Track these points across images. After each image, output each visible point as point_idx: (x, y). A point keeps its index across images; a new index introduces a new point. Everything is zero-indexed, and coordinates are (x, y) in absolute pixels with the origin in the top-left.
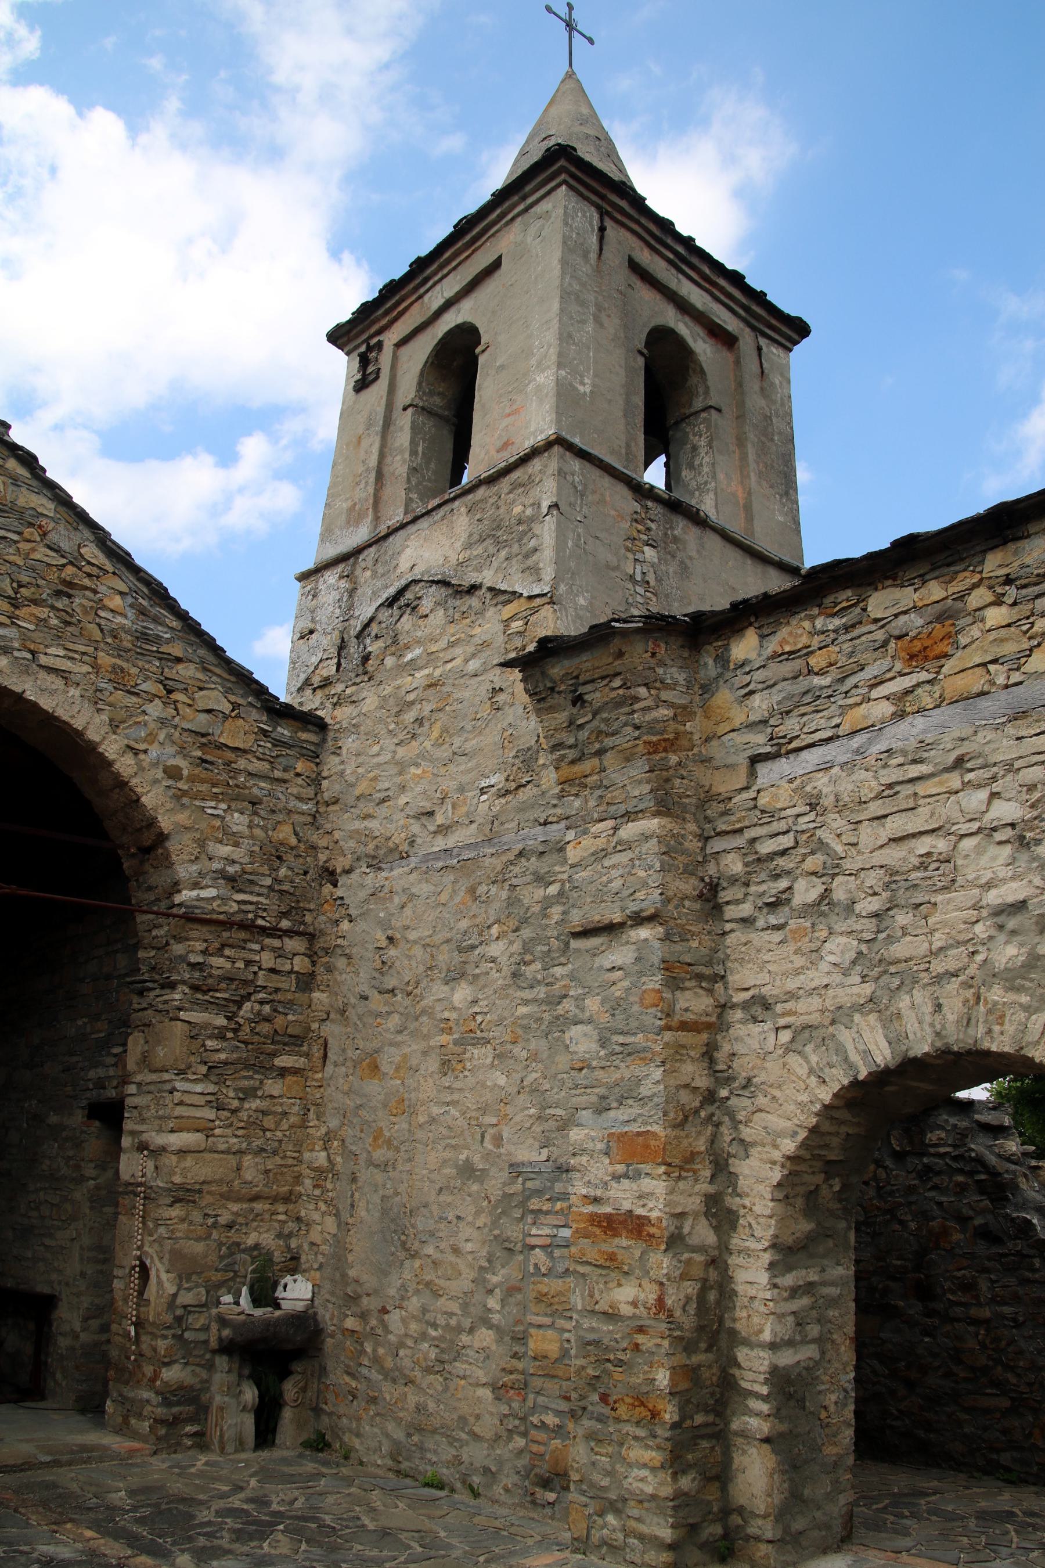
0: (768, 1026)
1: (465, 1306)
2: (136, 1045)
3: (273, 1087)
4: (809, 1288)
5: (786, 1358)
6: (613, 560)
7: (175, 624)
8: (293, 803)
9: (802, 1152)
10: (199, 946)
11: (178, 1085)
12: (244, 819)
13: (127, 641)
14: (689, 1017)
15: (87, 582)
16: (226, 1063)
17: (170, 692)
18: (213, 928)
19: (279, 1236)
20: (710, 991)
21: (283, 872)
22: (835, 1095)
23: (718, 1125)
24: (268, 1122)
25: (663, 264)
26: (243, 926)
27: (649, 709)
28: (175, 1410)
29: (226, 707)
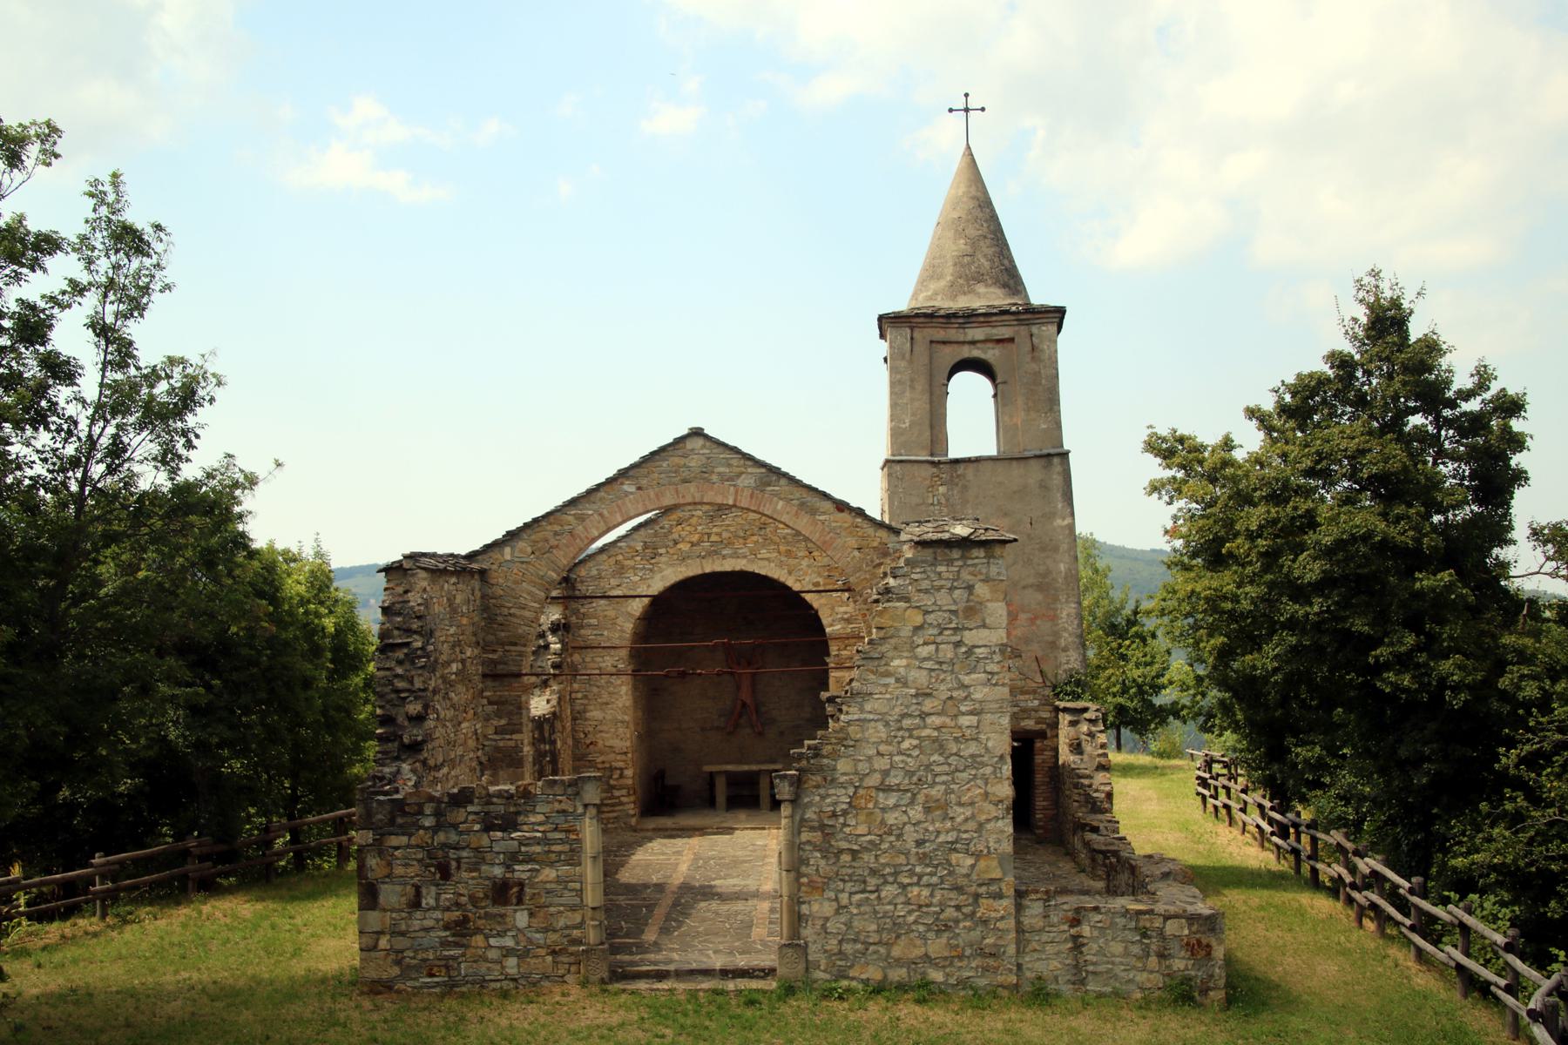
6: (919, 501)
13: (790, 538)
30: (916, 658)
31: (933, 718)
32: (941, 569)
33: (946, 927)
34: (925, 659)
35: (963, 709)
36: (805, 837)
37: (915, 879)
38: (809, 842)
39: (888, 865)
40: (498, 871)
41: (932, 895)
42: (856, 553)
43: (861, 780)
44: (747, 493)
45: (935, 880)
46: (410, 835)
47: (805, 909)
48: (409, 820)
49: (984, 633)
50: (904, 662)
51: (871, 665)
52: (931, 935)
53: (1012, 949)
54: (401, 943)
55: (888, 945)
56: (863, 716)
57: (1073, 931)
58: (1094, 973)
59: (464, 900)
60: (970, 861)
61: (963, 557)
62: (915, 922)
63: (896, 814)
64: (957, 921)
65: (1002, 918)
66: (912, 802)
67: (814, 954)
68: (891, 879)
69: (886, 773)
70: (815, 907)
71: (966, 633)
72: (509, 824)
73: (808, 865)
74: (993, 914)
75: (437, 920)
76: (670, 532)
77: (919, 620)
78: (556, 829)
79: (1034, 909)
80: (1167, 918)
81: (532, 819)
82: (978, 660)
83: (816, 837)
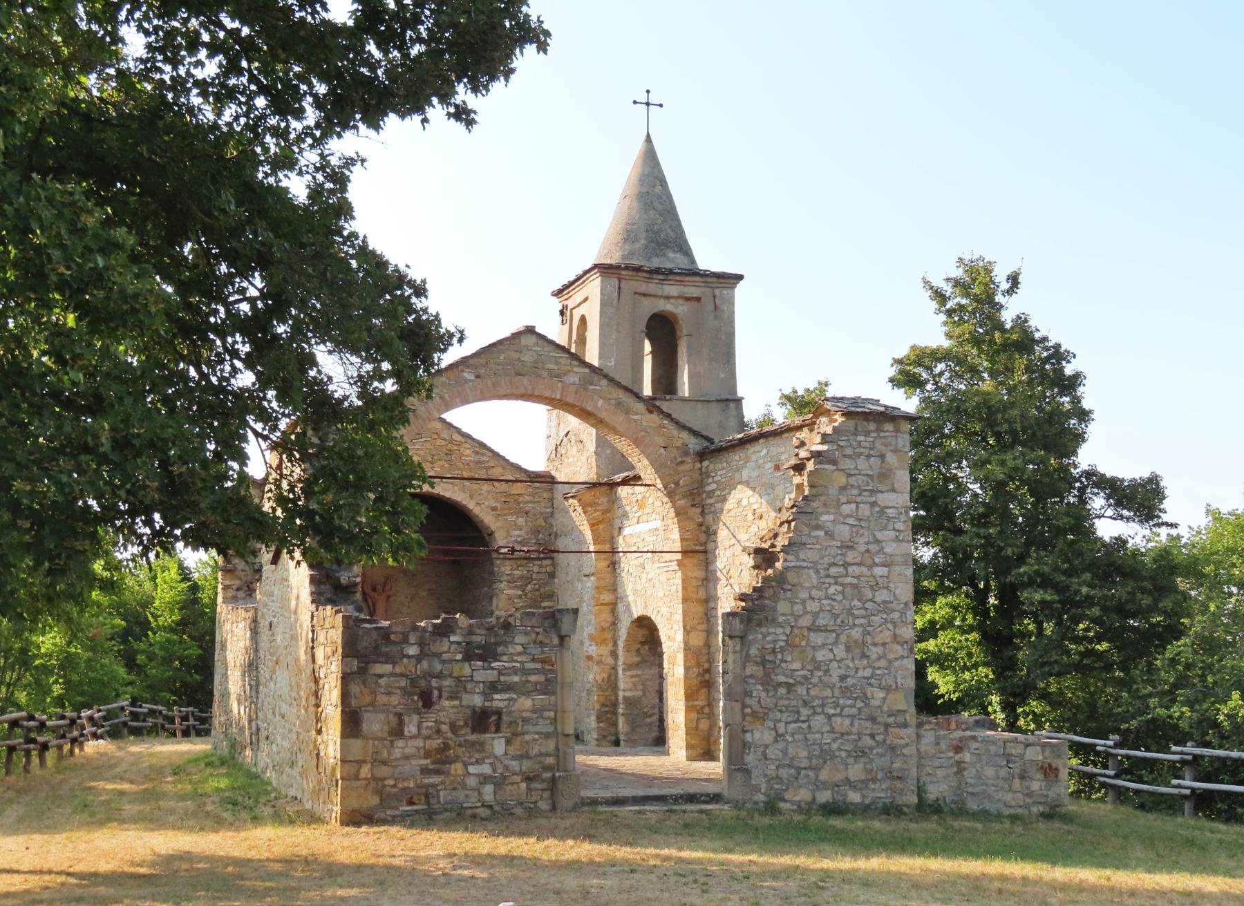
4: (638, 676)
5: (628, 694)
13: (472, 465)
30: (841, 515)
31: (854, 567)
32: (861, 438)
33: (861, 753)
34: (849, 516)
35: (877, 560)
36: (748, 671)
37: (838, 710)
38: (752, 676)
39: (818, 698)
40: (477, 701)
41: (852, 724)
43: (796, 620)
44: (572, 389)
45: (854, 711)
46: (394, 664)
47: (748, 737)
48: (395, 648)
49: (893, 495)
50: (831, 517)
51: (804, 518)
52: (851, 760)
53: (914, 773)
54: (384, 771)
55: (817, 769)
56: (798, 564)
57: (957, 757)
58: (973, 794)
59: (445, 728)
60: (881, 694)
61: (878, 430)
62: (839, 749)
63: (824, 652)
64: (871, 749)
65: (907, 745)
66: (836, 643)
67: (757, 778)
68: (819, 710)
69: (816, 615)
70: (757, 735)
71: (879, 495)
72: (487, 654)
73: (751, 696)
74: (901, 742)
75: (418, 749)
77: (843, 480)
78: (533, 660)
79: (928, 737)
80: (1027, 745)
81: (511, 650)
82: (889, 519)
83: (757, 671)
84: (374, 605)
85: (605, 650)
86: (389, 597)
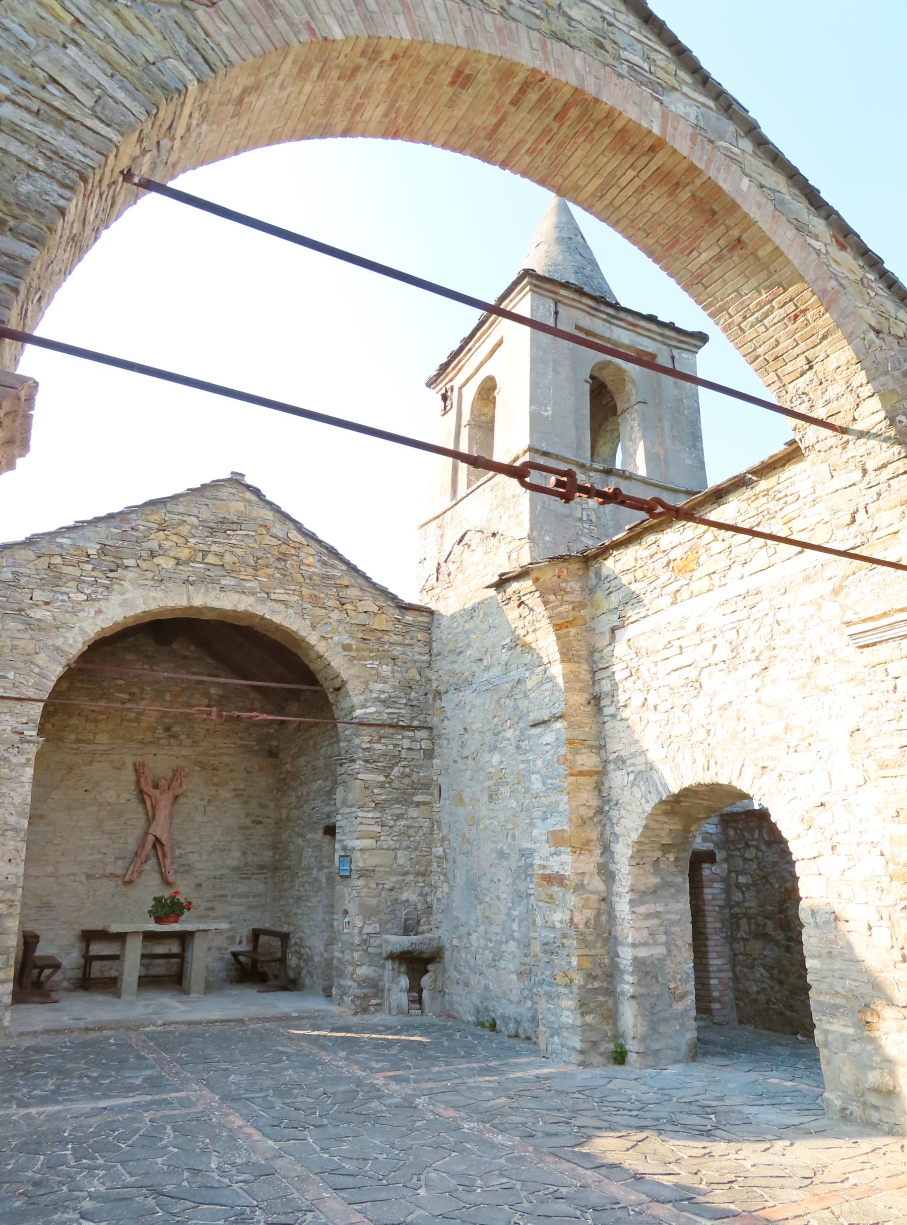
0: (624, 772)
1: (503, 929)
2: (339, 795)
3: (413, 812)
4: (657, 914)
5: (643, 953)
7: (344, 567)
8: (417, 657)
9: (642, 839)
10: (367, 739)
11: (360, 814)
12: (389, 668)
13: (317, 580)
14: (585, 768)
15: (293, 551)
16: (385, 801)
17: (343, 604)
18: (374, 728)
19: (420, 895)
20: (598, 754)
21: (413, 695)
22: (654, 808)
23: (604, 826)
24: (411, 832)
25: (600, 322)
26: (391, 726)
27: (557, 607)
28: (365, 991)
29: (376, 609)
42: (872, 334)
76: (146, 538)
84: (153, 807)
85: (589, 863)
86: (177, 797)
